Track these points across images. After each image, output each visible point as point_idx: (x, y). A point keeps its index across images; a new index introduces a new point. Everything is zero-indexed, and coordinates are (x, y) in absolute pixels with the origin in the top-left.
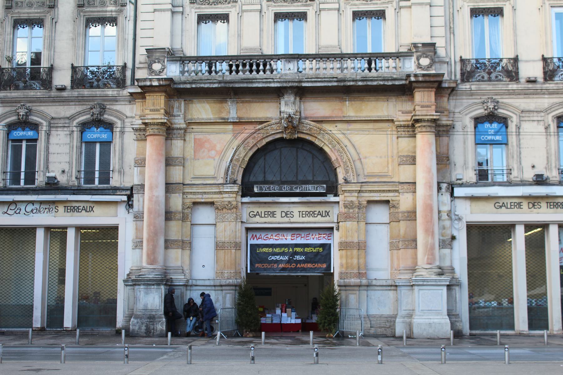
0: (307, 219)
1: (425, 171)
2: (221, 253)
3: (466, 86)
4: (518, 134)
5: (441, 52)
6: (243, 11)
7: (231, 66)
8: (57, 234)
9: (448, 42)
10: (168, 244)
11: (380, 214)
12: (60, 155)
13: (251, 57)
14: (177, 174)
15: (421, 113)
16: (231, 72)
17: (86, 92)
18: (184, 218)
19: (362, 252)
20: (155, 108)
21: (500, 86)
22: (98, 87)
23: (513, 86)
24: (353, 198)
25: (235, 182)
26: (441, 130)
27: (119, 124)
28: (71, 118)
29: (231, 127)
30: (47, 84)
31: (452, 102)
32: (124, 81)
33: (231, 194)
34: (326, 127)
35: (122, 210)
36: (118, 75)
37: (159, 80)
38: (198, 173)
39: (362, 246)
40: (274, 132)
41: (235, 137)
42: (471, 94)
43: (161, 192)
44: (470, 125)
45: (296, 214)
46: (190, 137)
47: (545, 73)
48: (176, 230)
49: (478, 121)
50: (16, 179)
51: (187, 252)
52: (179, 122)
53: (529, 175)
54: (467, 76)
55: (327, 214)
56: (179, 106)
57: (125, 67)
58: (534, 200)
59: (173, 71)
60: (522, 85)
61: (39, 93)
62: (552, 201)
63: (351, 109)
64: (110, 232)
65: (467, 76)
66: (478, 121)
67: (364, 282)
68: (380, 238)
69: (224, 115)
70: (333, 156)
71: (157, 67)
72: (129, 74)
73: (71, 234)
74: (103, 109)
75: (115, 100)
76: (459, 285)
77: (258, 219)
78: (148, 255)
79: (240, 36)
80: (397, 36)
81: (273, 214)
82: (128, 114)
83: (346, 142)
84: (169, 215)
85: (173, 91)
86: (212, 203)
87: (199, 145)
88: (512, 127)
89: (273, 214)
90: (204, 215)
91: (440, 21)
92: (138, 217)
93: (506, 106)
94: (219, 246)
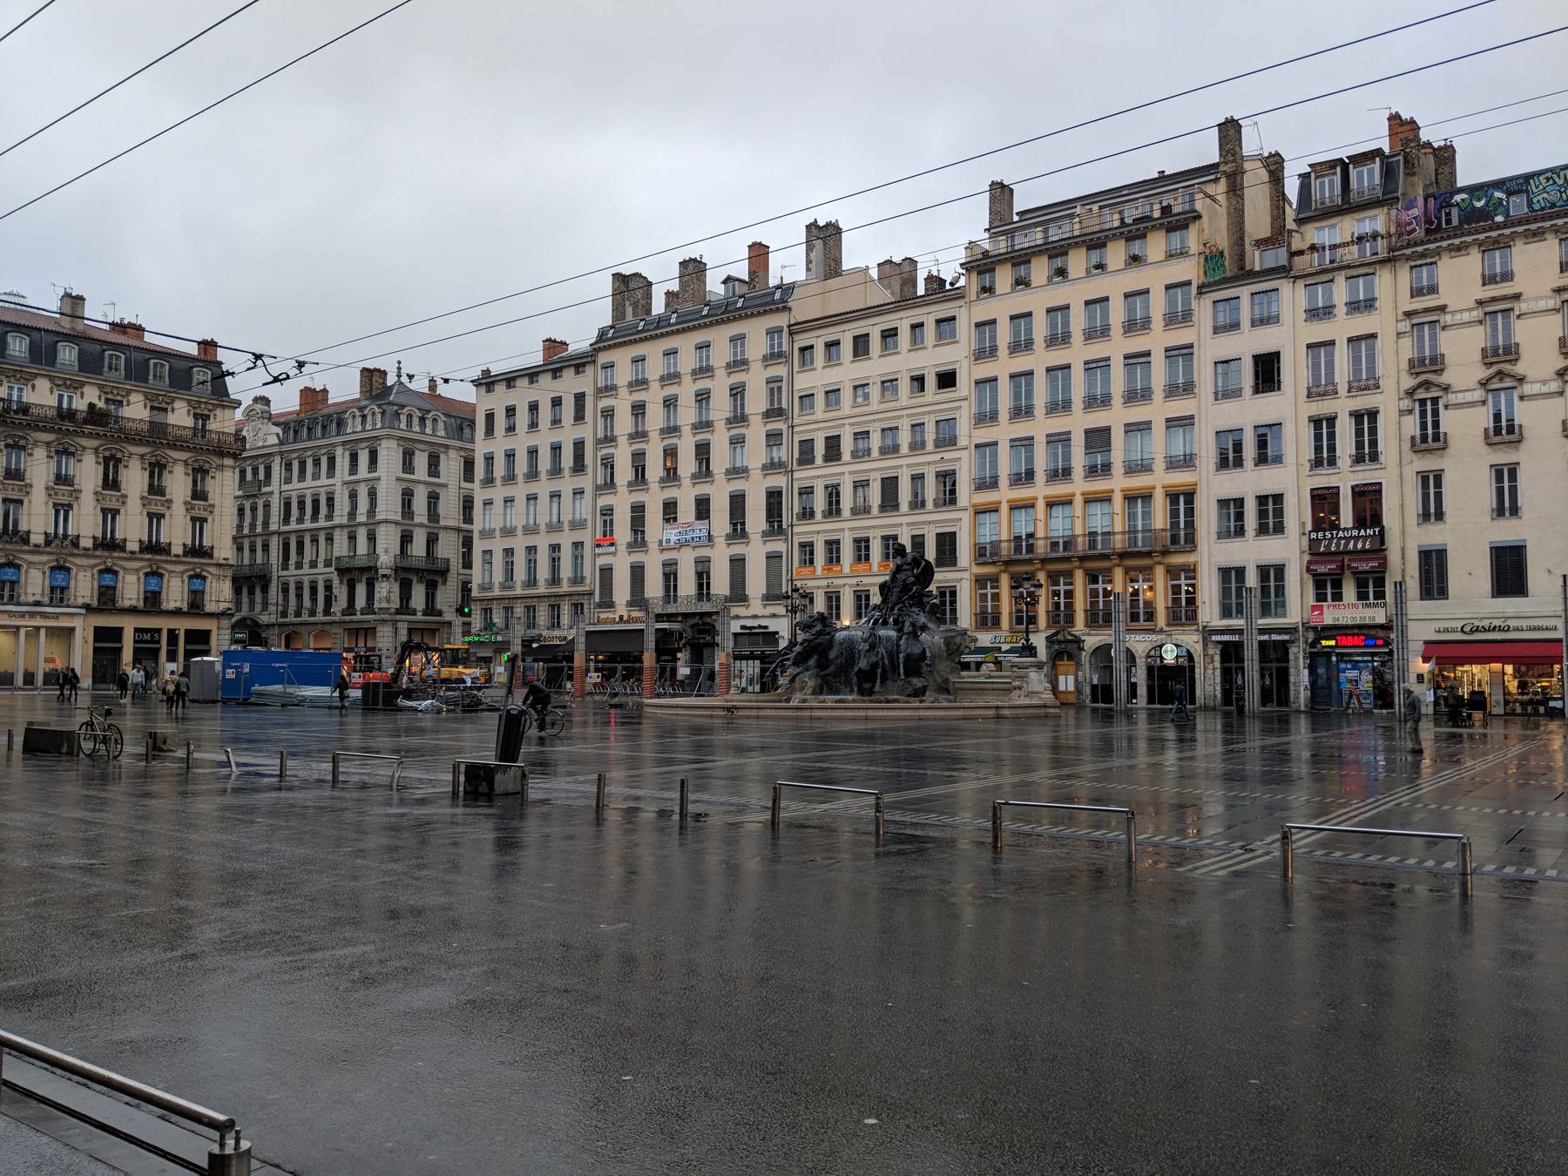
53: (31, 599)
58: (32, 615)
62: (44, 615)
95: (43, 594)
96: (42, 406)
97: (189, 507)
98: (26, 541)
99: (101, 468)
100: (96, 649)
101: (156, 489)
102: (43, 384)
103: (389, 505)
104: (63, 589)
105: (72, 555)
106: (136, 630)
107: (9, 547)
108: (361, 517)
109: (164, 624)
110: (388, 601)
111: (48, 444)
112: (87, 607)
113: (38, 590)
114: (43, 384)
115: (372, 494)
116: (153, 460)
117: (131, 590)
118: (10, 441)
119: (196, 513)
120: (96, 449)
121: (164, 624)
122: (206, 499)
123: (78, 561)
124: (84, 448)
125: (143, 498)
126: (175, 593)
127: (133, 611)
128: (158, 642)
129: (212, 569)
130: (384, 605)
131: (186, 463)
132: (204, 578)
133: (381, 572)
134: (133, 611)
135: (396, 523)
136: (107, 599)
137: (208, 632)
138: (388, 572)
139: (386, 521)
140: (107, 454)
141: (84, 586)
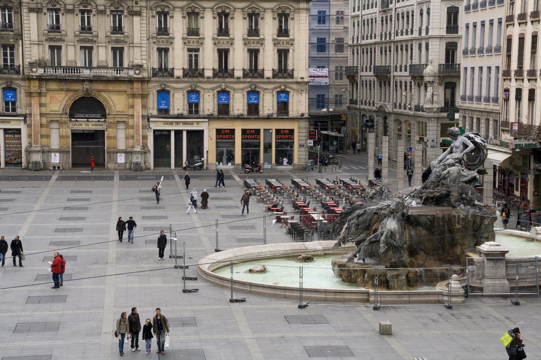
0: (94, 127)
1: (138, 111)
2: (62, 140)
3: (155, 79)
4: (173, 97)
5: (145, 66)
6: (67, 45)
7: (64, 70)
10: (42, 136)
11: (122, 126)
13: (72, 67)
14: (44, 110)
15: (135, 91)
16: (64, 72)
17: (4, 76)
18: (47, 127)
19: (115, 140)
20: (34, 86)
21: (167, 79)
22: (9, 74)
23: (171, 79)
24: (111, 120)
25: (66, 114)
26: (144, 96)
27: (19, 89)
29: (64, 92)
31: (149, 85)
32: (19, 72)
33: (65, 118)
34: (102, 93)
35: (22, 123)
36: (17, 69)
37: (36, 76)
38: (52, 109)
39: (115, 138)
40: (81, 95)
41: (66, 96)
42: (156, 82)
43: (38, 117)
44: (156, 94)
45: (90, 125)
46: (48, 96)
47: (183, 74)
48: (44, 131)
51: (49, 139)
52: (44, 90)
54: (155, 75)
55: (102, 125)
56: (44, 84)
57: (19, 66)
59: (41, 71)
60: (175, 79)
63: (111, 87)
65: (155, 75)
66: (159, 92)
67: (116, 151)
68: (121, 134)
69: (61, 88)
71: (34, 70)
72: (21, 68)
74: (12, 83)
75: (16, 79)
76: (149, 152)
77: (75, 126)
78: (34, 141)
79: (67, 55)
80: (129, 58)
81: (81, 125)
82: (22, 85)
83: (109, 99)
84: (42, 126)
85: (40, 79)
86: (58, 121)
87: (52, 98)
89: (81, 125)
90: (55, 125)
91: (144, 53)
92: (29, 126)
93: (169, 87)
94: (61, 137)
95: (184, 109)
97: (276, 43)
98: (172, 75)
99: (217, 21)
100: (217, 142)
101: (253, 31)
103: (438, 24)
104: (197, 105)
105: (200, 82)
106: (244, 132)
107: (161, 79)
108: (424, 34)
109: (261, 126)
110: (432, 102)
112: (210, 118)
113: (181, 108)
115: (428, 13)
116: (250, 11)
117: (239, 104)
118: (159, 10)
119: (281, 47)
120: (212, 9)
121: (261, 126)
122: (288, 36)
123: (204, 86)
124: (204, 9)
125: (244, 39)
126: (268, 104)
127: (239, 118)
128: (259, 139)
129: (294, 86)
130: (428, 106)
131: (273, 10)
132: (288, 93)
133: (427, 79)
134: (239, 118)
135: (441, 38)
136: (224, 110)
137: (291, 132)
138: (431, 79)
139: (431, 37)
140: (220, 11)
141: (209, 104)
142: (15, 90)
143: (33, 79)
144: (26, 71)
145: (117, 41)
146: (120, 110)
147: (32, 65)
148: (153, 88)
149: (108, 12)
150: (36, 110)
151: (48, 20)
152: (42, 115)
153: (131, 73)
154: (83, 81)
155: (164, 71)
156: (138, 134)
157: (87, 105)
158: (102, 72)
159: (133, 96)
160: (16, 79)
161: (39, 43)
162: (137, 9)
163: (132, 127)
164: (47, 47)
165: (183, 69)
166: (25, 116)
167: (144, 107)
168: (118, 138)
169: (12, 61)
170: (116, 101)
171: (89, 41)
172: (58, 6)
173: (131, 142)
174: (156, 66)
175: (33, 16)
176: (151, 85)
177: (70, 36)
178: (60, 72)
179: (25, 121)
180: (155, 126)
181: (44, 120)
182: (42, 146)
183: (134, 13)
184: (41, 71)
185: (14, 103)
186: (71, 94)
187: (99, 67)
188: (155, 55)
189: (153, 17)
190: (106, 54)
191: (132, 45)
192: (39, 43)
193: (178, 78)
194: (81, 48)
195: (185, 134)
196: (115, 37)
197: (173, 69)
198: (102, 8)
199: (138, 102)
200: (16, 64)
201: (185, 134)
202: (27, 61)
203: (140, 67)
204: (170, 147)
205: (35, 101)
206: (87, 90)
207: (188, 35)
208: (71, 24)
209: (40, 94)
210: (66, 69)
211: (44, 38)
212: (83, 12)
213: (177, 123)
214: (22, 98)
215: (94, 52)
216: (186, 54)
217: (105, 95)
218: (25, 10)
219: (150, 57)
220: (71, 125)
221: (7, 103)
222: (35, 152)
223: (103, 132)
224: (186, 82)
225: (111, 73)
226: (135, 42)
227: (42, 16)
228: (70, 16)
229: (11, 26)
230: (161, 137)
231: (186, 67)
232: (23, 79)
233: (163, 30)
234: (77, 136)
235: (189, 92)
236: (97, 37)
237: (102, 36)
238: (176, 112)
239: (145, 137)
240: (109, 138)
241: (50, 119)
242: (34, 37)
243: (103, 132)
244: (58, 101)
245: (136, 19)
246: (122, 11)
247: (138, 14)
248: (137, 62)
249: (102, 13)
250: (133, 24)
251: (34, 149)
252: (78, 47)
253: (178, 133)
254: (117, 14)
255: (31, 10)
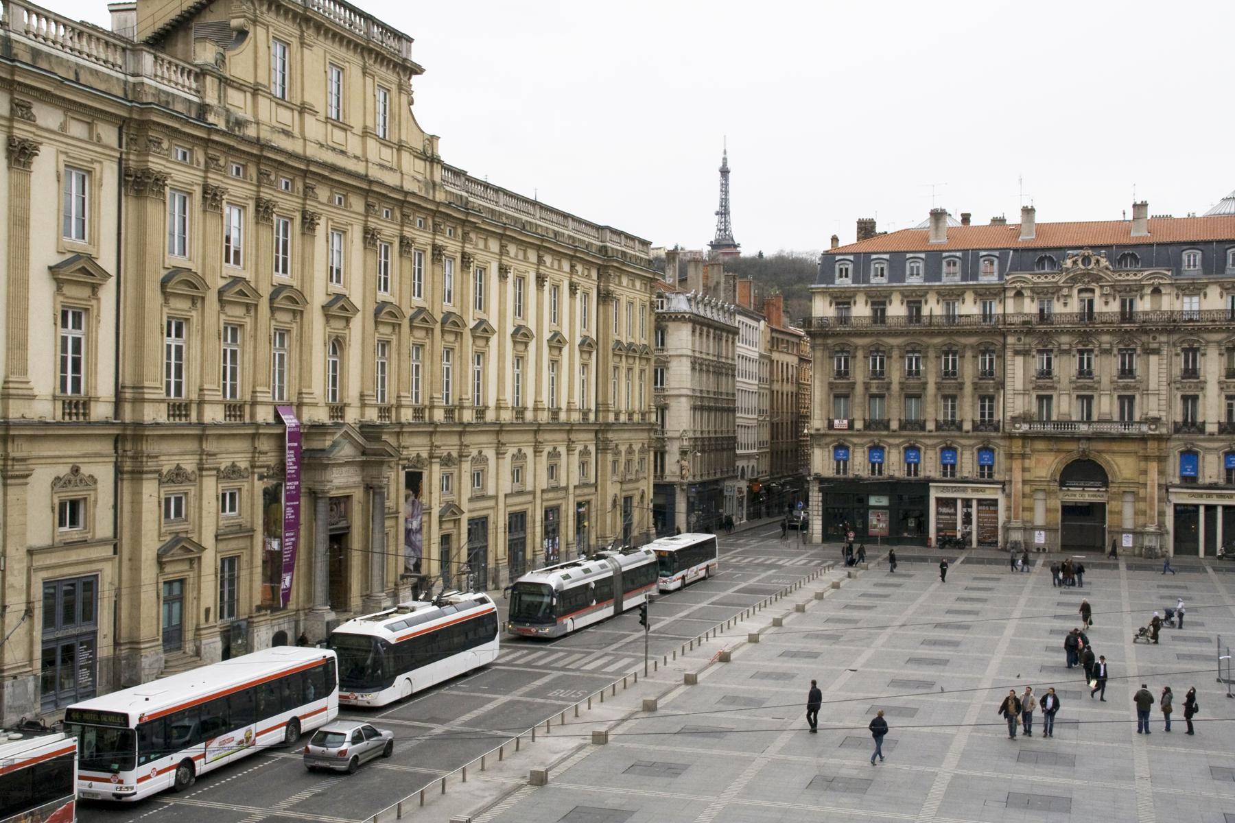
1: (1153, 476)
5: (1164, 419)
8: (967, 503)
9: (1168, 413)
11: (1129, 498)
12: (967, 464)
14: (1028, 476)
18: (1031, 496)
20: (1017, 447)
21: (1194, 437)
23: (1202, 437)
26: (1161, 459)
28: (972, 446)
30: (960, 428)
33: (1055, 486)
39: (1120, 513)
40: (1075, 456)
43: (1020, 485)
46: (1033, 460)
48: (1027, 502)
49: (1182, 453)
50: (945, 474)
52: (1028, 450)
54: (1177, 431)
59: (1025, 427)
61: (957, 433)
63: (1115, 447)
64: (995, 502)
65: (1177, 431)
66: (1182, 453)
68: (1128, 510)
70: (1106, 469)
73: (974, 503)
74: (989, 442)
76: (1167, 533)
84: (1024, 496)
85: (1024, 437)
87: (1038, 461)
88: (1200, 457)
90: (1041, 496)
91: (1163, 402)
92: (1008, 496)
93: (1198, 446)
94: (1048, 510)
95: (1219, 477)
96: (1210, 312)
102: (1213, 292)
107: (1186, 436)
111: (1219, 343)
114: (1213, 292)
118: (1186, 345)
142: (992, 451)
143: (1015, 437)
144: (1007, 428)
145: (1126, 387)
146: (1128, 476)
147: (1014, 420)
148: (1175, 449)
149: (1115, 351)
150: (1017, 476)
151: (1037, 363)
152: (1024, 482)
153: (1145, 428)
154: (1079, 439)
155: (1191, 425)
156: (1152, 509)
157: (1086, 470)
158: (1105, 428)
159: (1146, 458)
160: (994, 438)
161: (1025, 393)
162: (1156, 346)
163: (1144, 500)
164: (1034, 396)
165: (1219, 423)
166: (1004, 483)
167: (1161, 473)
168: (1125, 514)
169: (991, 415)
170: (1122, 466)
171: (1089, 388)
172: (1050, 347)
173: (1141, 520)
174: (1179, 419)
175: (1019, 360)
176: (1172, 444)
177: (1065, 382)
178: (1049, 428)
179: (1004, 490)
180: (1175, 499)
181: (1027, 489)
182: (1024, 522)
183: (1148, 352)
184: (1025, 427)
185: (990, 468)
186: (1062, 456)
187: (1099, 421)
188: (1178, 406)
189: (1177, 355)
190: (1111, 404)
191: (1146, 392)
192: (1025, 393)
193: (1212, 434)
194: (1078, 397)
195: (1220, 510)
196: (1122, 382)
197: (1204, 423)
198: (1107, 346)
199: (1153, 467)
200: (995, 418)
201: (1220, 510)
202: (1009, 414)
203: (1156, 421)
204: (1197, 529)
205: (1016, 465)
206: (1084, 451)
207: (1227, 377)
208: (1065, 368)
209: (1023, 456)
210: (1058, 423)
211: (1031, 386)
212: (1081, 352)
213: (1209, 496)
214: (1000, 460)
215: (1095, 403)
216: (1224, 402)
217: (1107, 457)
218: (1009, 353)
219: (1170, 407)
220: (1061, 495)
221: (982, 467)
222: (1015, 529)
223: (1103, 505)
224: (1223, 440)
225: (1117, 429)
226: (1151, 387)
227: (1030, 359)
228: (1065, 358)
229: (991, 373)
230: (1185, 515)
231: (1223, 419)
232: (1004, 438)
233: (1191, 373)
234: (1069, 510)
235: (1227, 454)
236: (1099, 382)
237: (1105, 381)
238: (1208, 481)
239: (1162, 514)
240: (1111, 512)
241: (1034, 487)
242: (1019, 385)
243: (1103, 505)
244: (1046, 465)
245: (1153, 359)
246: (1134, 350)
247: (1157, 352)
248: (1153, 413)
249: (1107, 352)
250: (1148, 365)
251: (1013, 524)
252: (1074, 396)
253: (1210, 509)
254: (1127, 353)
255: (1017, 353)
